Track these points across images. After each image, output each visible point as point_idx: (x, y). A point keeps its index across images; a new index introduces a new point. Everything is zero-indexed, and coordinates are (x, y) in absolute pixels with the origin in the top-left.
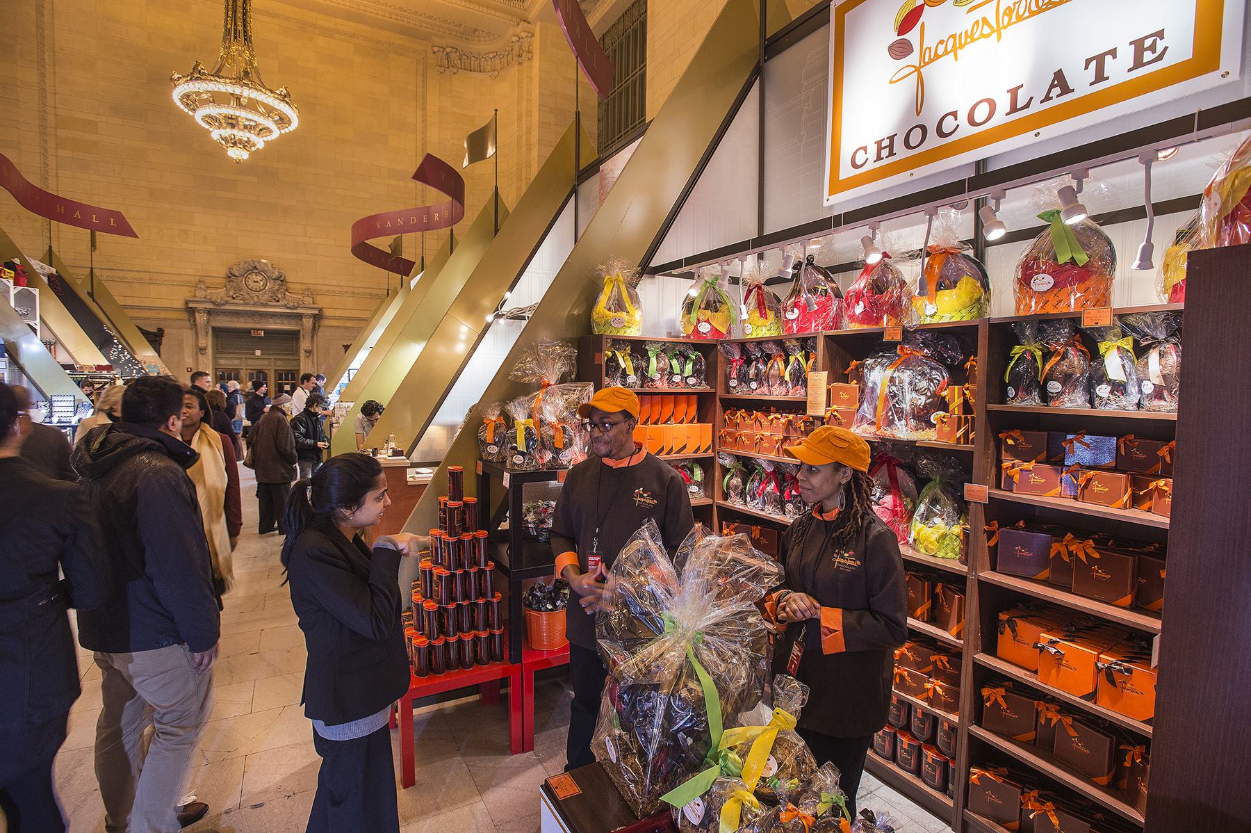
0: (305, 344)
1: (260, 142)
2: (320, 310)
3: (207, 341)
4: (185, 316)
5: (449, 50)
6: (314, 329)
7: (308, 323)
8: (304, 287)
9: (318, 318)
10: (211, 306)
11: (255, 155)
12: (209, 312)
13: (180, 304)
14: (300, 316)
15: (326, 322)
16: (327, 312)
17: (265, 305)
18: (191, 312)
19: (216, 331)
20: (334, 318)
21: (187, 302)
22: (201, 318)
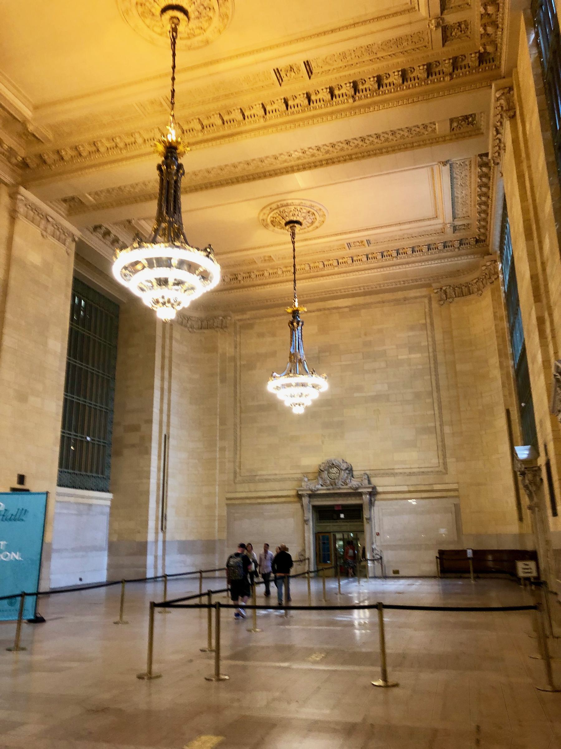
0: (366, 515)
1: (308, 403)
2: (374, 488)
3: (309, 515)
4: (296, 499)
5: (444, 288)
6: (371, 504)
7: (366, 498)
8: (363, 472)
9: (373, 493)
10: (310, 492)
11: (307, 408)
12: (310, 496)
13: (293, 493)
14: (360, 494)
15: (379, 497)
16: (379, 489)
17: (340, 489)
18: (299, 496)
19: (314, 507)
20: (384, 493)
21: (297, 492)
22: (305, 500)
